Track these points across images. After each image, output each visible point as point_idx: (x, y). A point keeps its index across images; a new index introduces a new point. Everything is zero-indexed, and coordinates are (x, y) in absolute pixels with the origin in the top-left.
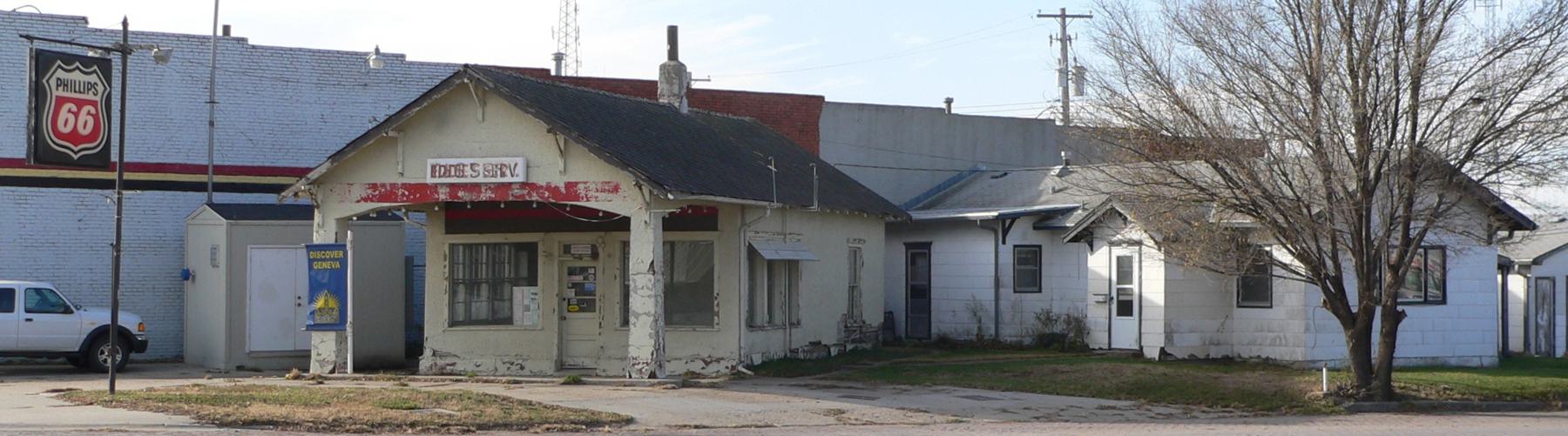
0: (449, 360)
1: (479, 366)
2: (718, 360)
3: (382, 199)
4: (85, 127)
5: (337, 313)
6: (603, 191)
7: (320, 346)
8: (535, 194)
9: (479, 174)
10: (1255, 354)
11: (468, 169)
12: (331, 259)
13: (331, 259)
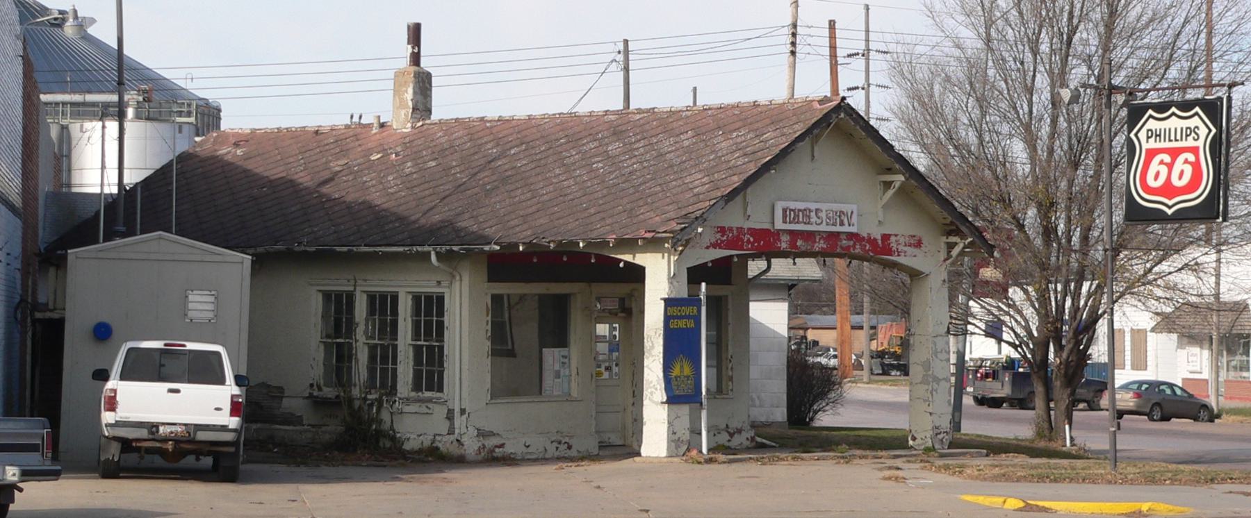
0: (494, 441)
1: (528, 447)
2: (739, 431)
3: (730, 245)
5: (693, 382)
9: (822, 223)
11: (813, 214)
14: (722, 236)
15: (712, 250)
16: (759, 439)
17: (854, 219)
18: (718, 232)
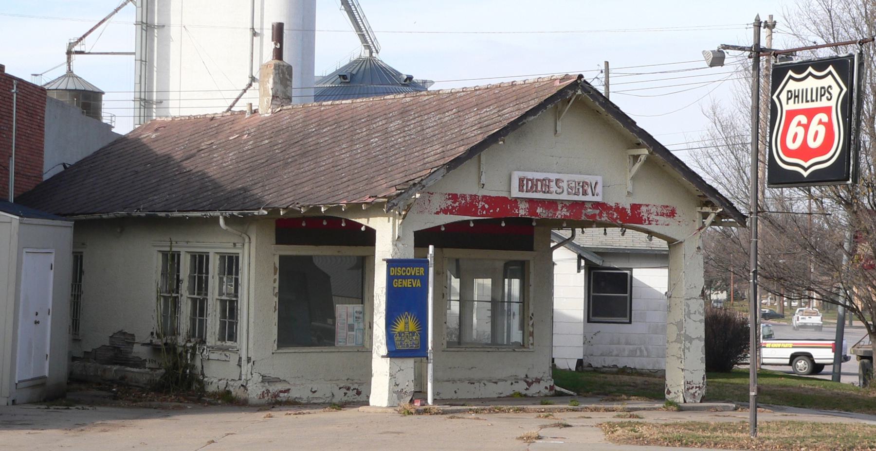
0: (280, 387)
1: (314, 392)
2: (538, 381)
3: (462, 211)
4: (815, 139)
5: (418, 338)
6: (662, 215)
7: (397, 375)
8: (605, 215)
9: (563, 191)
10: (611, 364)
11: (553, 184)
12: (411, 277)
13: (411, 277)
14: (454, 203)
15: (442, 215)
16: (558, 388)
17: (599, 189)
18: (449, 199)
